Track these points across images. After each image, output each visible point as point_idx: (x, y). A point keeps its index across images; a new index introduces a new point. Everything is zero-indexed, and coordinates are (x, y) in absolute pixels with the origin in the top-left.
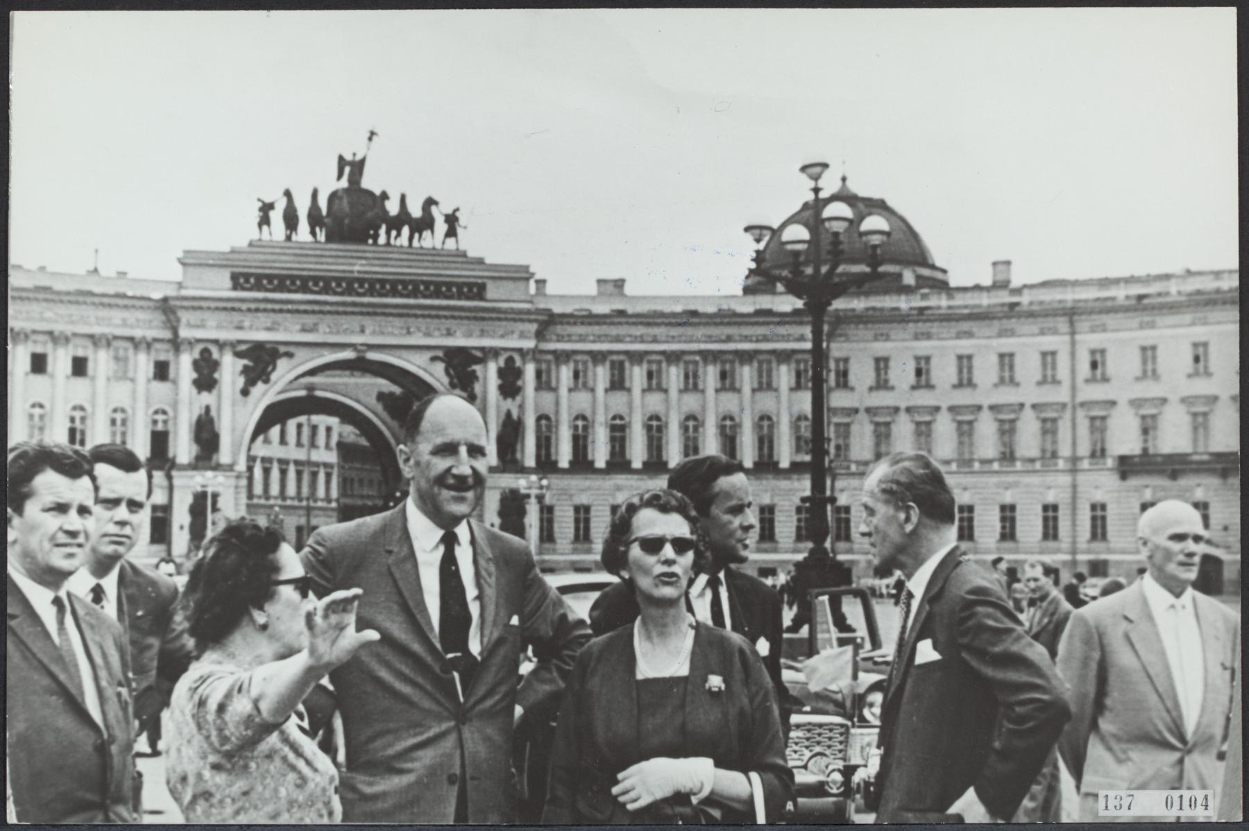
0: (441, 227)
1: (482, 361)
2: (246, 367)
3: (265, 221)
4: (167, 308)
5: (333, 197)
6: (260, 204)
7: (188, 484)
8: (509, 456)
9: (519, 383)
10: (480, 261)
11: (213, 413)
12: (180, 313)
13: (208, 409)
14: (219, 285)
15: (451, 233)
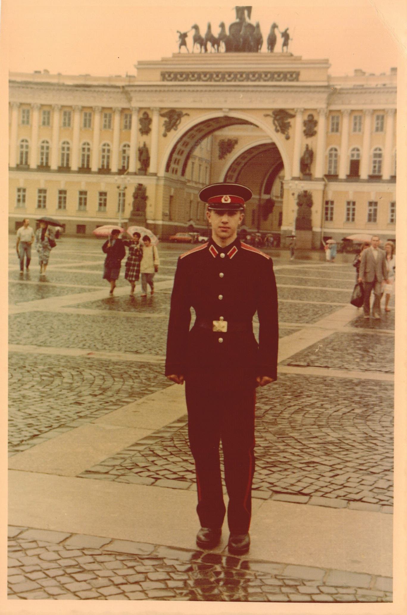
0: (280, 40)
1: (293, 116)
2: (165, 121)
3: (183, 43)
4: (125, 91)
5: (232, 26)
6: (179, 35)
7: (131, 182)
8: (307, 171)
9: (316, 129)
10: (299, 59)
11: (148, 146)
12: (132, 94)
13: (145, 145)
14: (155, 79)
15: (285, 44)
